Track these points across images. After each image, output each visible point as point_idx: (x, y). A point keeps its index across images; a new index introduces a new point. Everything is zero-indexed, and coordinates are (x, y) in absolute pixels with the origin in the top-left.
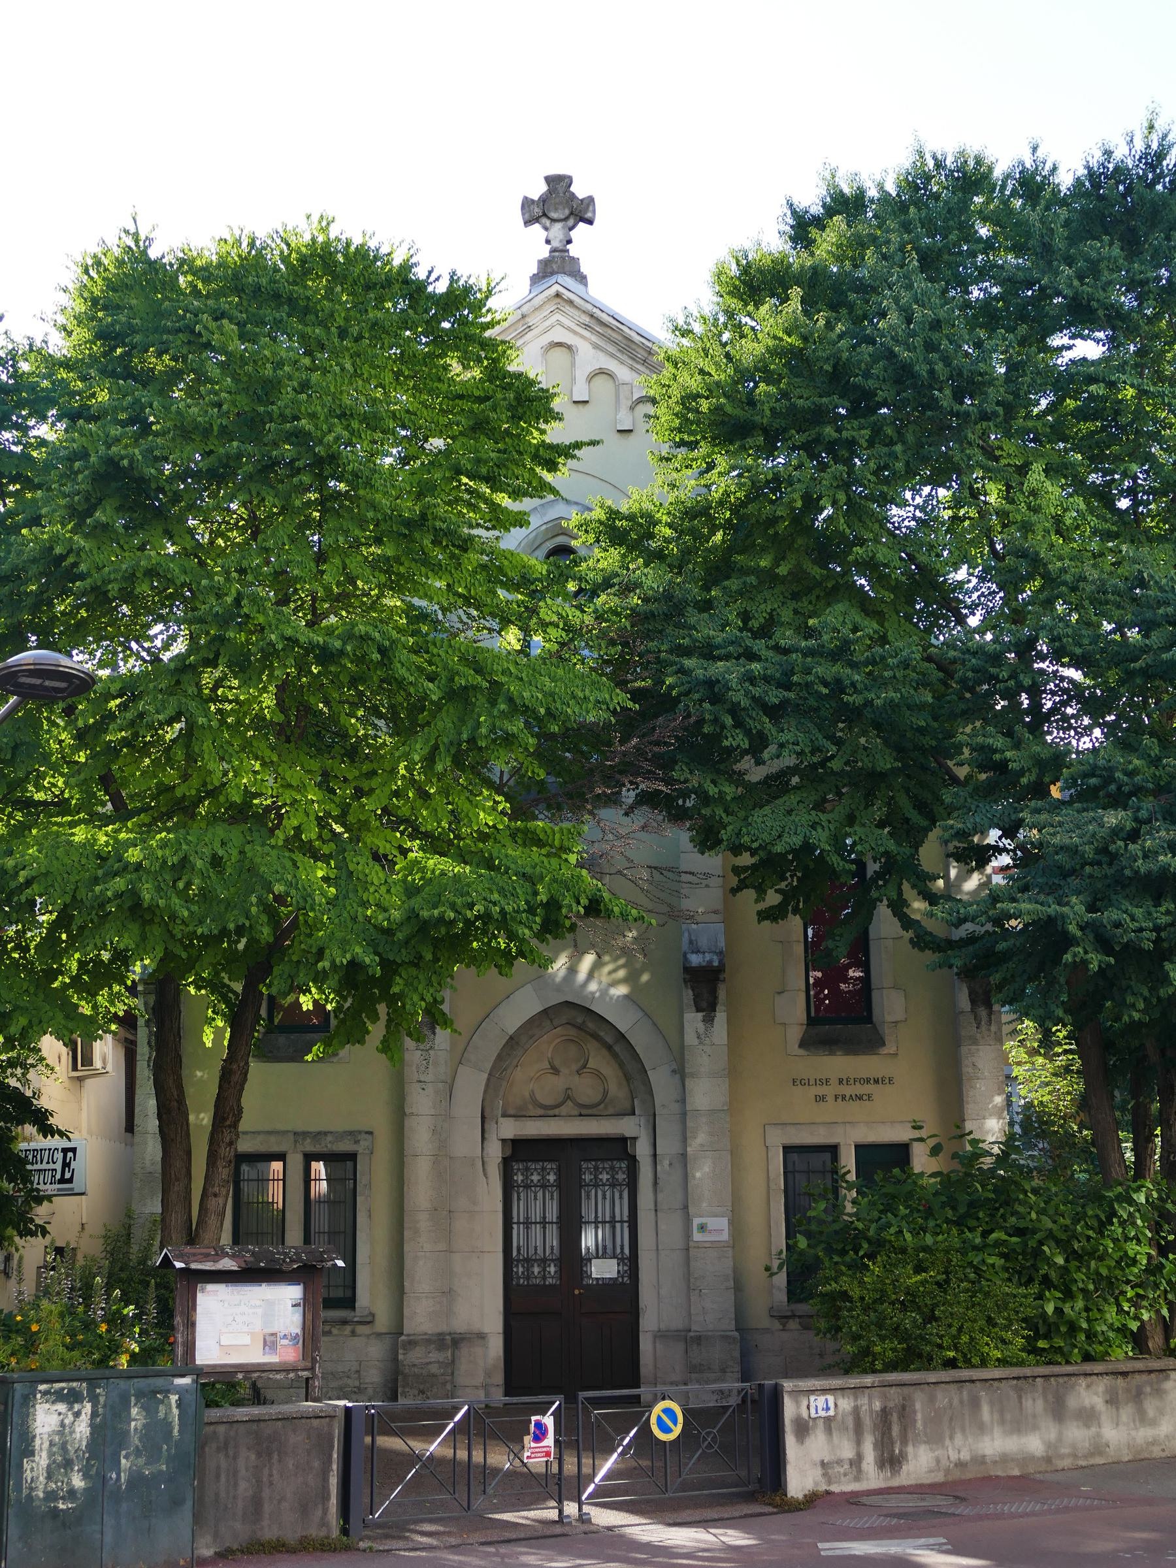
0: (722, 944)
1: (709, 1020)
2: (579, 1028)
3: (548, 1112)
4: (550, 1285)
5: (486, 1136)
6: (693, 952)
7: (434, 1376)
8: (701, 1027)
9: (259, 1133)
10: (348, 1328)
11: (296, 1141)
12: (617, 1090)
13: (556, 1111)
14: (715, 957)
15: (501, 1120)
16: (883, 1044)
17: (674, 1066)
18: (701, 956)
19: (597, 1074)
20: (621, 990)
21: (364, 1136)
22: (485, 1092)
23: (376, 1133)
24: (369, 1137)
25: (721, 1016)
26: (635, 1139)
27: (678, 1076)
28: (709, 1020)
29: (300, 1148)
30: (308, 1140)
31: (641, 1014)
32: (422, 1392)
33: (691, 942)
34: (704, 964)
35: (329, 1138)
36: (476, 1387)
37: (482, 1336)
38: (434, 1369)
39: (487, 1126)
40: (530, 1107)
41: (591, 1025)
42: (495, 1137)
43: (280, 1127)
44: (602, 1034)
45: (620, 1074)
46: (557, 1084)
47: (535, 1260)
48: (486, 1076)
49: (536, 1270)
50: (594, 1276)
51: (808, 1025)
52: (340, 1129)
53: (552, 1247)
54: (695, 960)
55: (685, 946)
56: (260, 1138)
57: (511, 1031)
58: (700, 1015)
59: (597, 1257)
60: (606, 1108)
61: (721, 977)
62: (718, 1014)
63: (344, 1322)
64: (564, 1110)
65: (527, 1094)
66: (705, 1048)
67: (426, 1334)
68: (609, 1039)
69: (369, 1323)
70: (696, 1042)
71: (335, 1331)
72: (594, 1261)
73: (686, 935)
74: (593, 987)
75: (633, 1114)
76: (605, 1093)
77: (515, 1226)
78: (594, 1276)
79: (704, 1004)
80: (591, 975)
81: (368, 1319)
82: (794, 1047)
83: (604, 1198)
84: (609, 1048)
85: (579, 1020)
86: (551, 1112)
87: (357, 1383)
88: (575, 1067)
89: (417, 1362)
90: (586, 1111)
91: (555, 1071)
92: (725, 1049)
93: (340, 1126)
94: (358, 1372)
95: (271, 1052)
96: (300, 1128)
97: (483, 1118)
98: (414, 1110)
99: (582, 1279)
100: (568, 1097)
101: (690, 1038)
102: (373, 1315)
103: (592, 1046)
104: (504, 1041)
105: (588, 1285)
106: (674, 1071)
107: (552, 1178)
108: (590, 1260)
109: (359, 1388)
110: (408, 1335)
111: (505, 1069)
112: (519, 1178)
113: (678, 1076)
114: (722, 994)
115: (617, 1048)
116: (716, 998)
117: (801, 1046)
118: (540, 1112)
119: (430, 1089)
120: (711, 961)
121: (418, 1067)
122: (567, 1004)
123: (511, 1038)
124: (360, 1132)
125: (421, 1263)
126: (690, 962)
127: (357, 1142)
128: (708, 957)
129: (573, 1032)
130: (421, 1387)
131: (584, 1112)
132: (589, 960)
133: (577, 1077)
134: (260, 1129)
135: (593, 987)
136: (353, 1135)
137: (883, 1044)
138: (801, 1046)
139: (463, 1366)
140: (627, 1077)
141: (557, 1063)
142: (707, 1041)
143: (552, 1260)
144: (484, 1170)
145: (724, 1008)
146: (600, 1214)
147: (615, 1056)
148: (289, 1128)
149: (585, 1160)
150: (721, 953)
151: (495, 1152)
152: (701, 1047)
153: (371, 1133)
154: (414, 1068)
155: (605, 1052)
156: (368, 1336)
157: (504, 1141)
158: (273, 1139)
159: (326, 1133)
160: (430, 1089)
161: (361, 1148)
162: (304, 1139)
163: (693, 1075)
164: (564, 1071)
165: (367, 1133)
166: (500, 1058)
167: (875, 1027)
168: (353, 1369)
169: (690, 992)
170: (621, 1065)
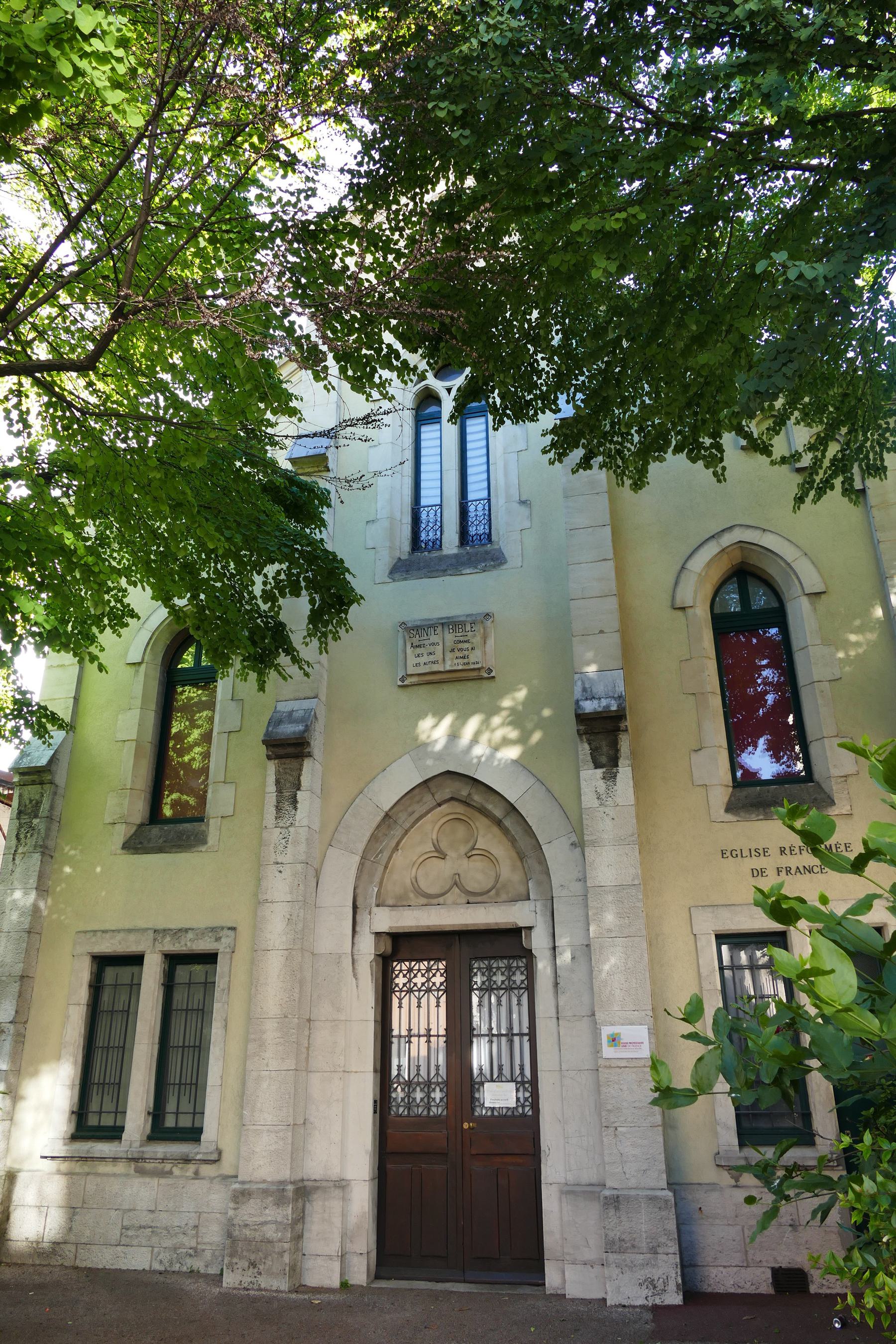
0: (621, 688)
1: (610, 777)
2: (466, 803)
3: (431, 899)
4: (435, 1116)
5: (358, 929)
6: (587, 699)
7: (270, 1242)
8: (601, 785)
9: (119, 931)
10: (192, 1168)
11: (155, 940)
12: (508, 870)
13: (441, 900)
14: (613, 702)
15: (375, 910)
16: (832, 803)
17: (574, 838)
18: (596, 702)
19: (486, 855)
20: (513, 753)
21: (225, 931)
22: (358, 878)
23: (239, 929)
24: (231, 933)
25: (624, 771)
26: (530, 928)
27: (578, 850)
28: (610, 777)
29: (159, 947)
30: (168, 939)
31: (532, 780)
32: (253, 1265)
33: (584, 690)
34: (600, 709)
35: (190, 935)
36: (330, 1257)
37: (342, 1185)
38: (270, 1232)
39: (358, 918)
40: (412, 895)
41: (477, 798)
42: (367, 930)
43: (142, 924)
44: (490, 807)
45: (514, 855)
46: (443, 869)
47: (418, 1084)
48: (357, 859)
49: (419, 1095)
50: (487, 1105)
51: (734, 787)
52: (203, 925)
53: (437, 1067)
54: (589, 706)
55: (578, 689)
56: (119, 936)
57: (386, 807)
58: (600, 772)
59: (492, 1081)
60: (497, 894)
61: (622, 725)
62: (620, 769)
63: (187, 1160)
64: (449, 897)
65: (408, 882)
66: (606, 810)
67: (264, 1181)
68: (498, 813)
69: (215, 1161)
70: (596, 803)
71: (176, 1171)
72: (486, 1085)
73: (579, 683)
74: (479, 750)
75: (528, 898)
76: (498, 877)
77: (395, 1040)
78: (487, 1105)
79: (604, 759)
80: (475, 741)
81: (214, 1157)
82: (719, 812)
83: (499, 1003)
84: (499, 823)
85: (464, 793)
86: (435, 901)
87: (193, 1244)
88: (463, 849)
89: (250, 1221)
90: (473, 898)
91: (443, 856)
92: (632, 810)
93: (201, 922)
94: (196, 1227)
95: (141, 843)
96: (160, 926)
97: (355, 908)
98: (269, 897)
99: (473, 1110)
100: (457, 883)
101: (589, 800)
102: (220, 1153)
103: (481, 823)
104: (379, 818)
105: (481, 1116)
106: (573, 844)
107: (438, 979)
108: (482, 1084)
109: (195, 1249)
110: (243, 1183)
111: (381, 852)
112: (400, 981)
113: (578, 850)
114: (625, 744)
115: (507, 823)
116: (617, 751)
117: (728, 809)
118: (424, 901)
119: (287, 871)
120: (608, 706)
121: (275, 847)
122: (450, 774)
123: (387, 815)
124: (223, 928)
125: (265, 1085)
126: (583, 709)
127: (218, 939)
128: (604, 702)
129: (459, 808)
130: (253, 1257)
131: (472, 899)
132: (473, 724)
133: (465, 861)
134: (120, 926)
135: (479, 750)
136: (215, 931)
137: (832, 803)
138: (728, 809)
139: (314, 1227)
140: (522, 857)
141: (443, 845)
142: (610, 802)
143: (438, 1084)
144: (354, 968)
145: (628, 762)
146: (494, 1025)
147: (506, 831)
148: (150, 925)
149: (477, 959)
150: (620, 697)
151: (367, 948)
152: (602, 809)
153: (233, 929)
154: (271, 848)
155: (495, 830)
156: (212, 1179)
157: (378, 934)
158: (132, 937)
159: (187, 930)
160: (287, 871)
161: (221, 947)
162: (164, 937)
163: (594, 843)
164: (451, 854)
165: (229, 929)
166: (374, 838)
167: (819, 785)
168: (192, 1223)
169: (587, 746)
170: (513, 841)
